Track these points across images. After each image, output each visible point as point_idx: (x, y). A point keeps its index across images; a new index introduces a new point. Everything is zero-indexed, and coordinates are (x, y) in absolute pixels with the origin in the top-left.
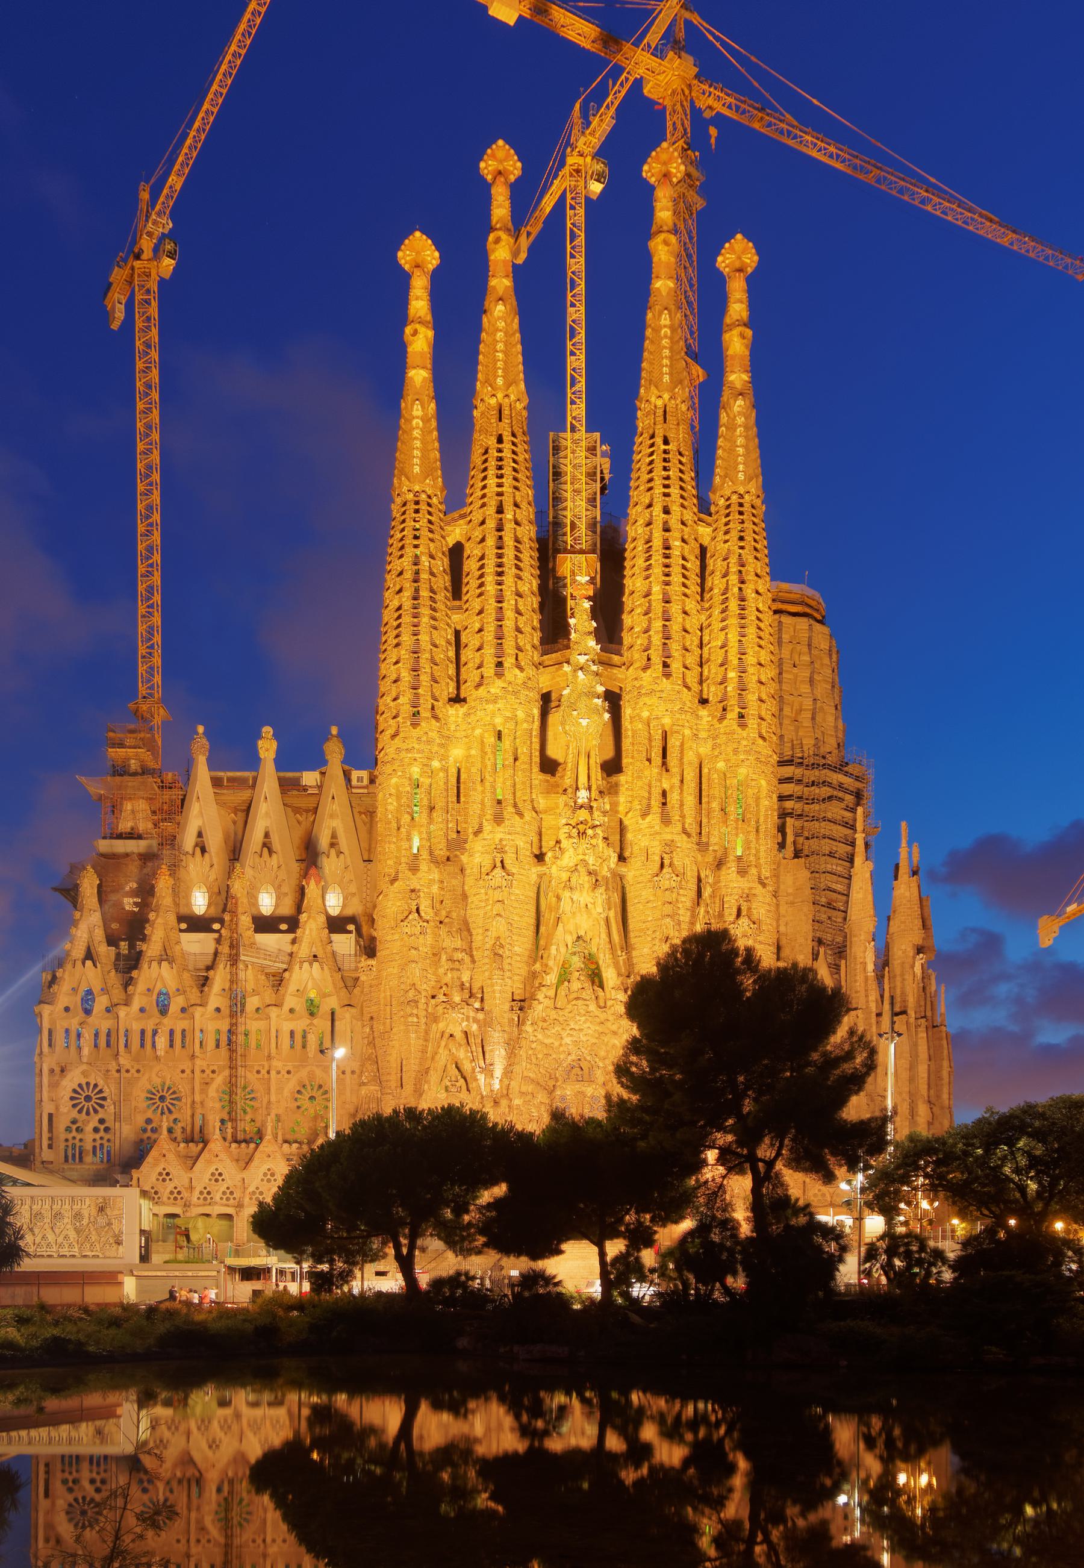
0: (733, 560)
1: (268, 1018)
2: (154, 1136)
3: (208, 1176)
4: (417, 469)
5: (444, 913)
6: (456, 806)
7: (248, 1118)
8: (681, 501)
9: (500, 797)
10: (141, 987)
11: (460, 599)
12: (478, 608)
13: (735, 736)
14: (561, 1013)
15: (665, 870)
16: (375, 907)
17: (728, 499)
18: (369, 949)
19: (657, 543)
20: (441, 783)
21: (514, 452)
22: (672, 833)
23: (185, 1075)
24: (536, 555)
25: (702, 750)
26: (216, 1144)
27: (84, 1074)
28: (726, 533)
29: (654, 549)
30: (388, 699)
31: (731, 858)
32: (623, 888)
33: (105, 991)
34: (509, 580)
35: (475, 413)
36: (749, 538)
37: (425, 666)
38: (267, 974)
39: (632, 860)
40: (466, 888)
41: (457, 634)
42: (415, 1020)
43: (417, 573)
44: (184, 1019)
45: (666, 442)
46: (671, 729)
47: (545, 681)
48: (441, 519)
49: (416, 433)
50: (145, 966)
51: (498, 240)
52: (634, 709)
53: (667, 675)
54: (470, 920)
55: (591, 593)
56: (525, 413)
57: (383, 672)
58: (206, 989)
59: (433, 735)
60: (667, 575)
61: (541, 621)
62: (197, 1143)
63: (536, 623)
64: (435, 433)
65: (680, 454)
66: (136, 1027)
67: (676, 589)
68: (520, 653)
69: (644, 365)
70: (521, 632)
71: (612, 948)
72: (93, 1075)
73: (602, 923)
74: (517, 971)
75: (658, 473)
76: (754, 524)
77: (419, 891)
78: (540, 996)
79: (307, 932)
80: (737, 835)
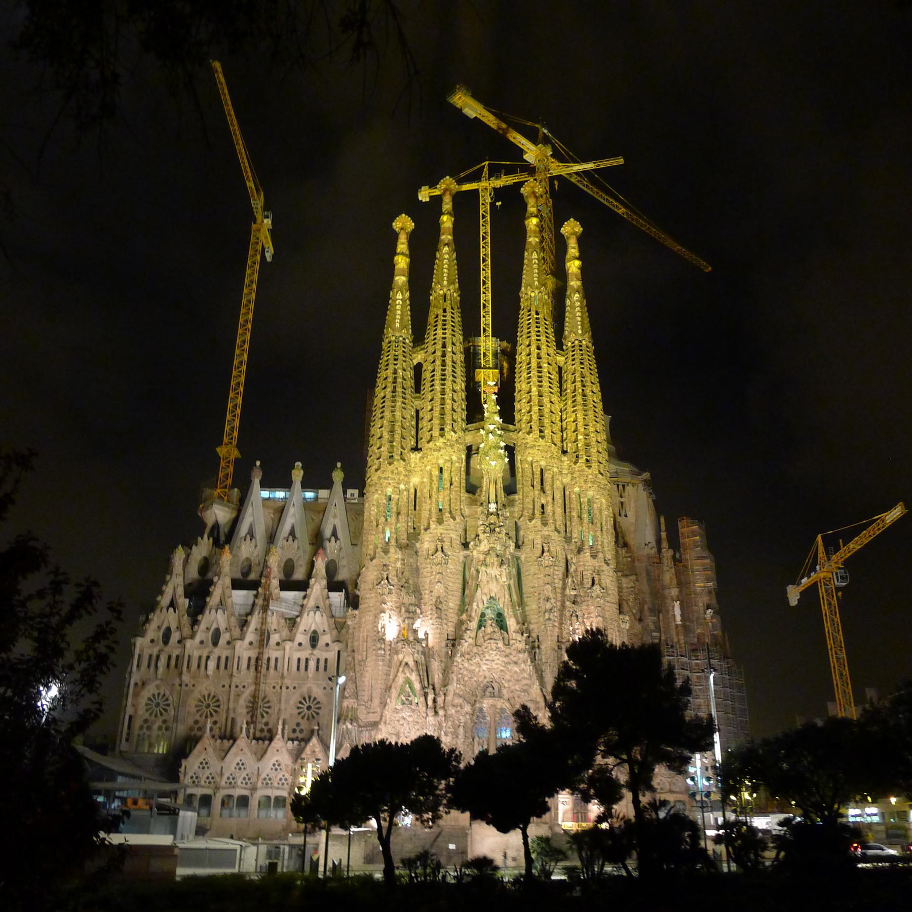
0: (578, 375)
1: (284, 649)
2: (199, 733)
3: (234, 765)
4: (398, 325)
5: (404, 580)
6: (413, 512)
7: (264, 720)
9: (441, 507)
10: (203, 626)
11: (420, 393)
12: (430, 398)
14: (479, 648)
15: (545, 554)
16: (359, 575)
17: (573, 343)
18: (353, 602)
19: (534, 365)
20: (405, 499)
21: (452, 317)
22: (548, 531)
23: (224, 689)
24: (464, 370)
25: (565, 481)
26: (242, 742)
27: (158, 687)
28: (573, 360)
30: (375, 448)
31: (586, 547)
32: (518, 565)
33: (179, 628)
34: (448, 383)
35: (431, 297)
36: (586, 363)
37: (398, 430)
38: (286, 619)
39: (524, 548)
40: (419, 564)
41: (417, 412)
42: (383, 652)
43: (395, 378)
44: (229, 649)
45: (537, 313)
46: (545, 468)
47: (469, 439)
49: (398, 307)
50: (207, 612)
52: (522, 456)
53: (543, 437)
54: (421, 585)
55: (496, 391)
56: (459, 298)
57: (372, 432)
58: (245, 628)
60: (541, 382)
61: (467, 406)
62: (228, 740)
63: (464, 407)
64: (409, 307)
65: (545, 320)
66: (196, 654)
67: (546, 389)
68: (454, 423)
69: (524, 276)
70: (455, 411)
71: (513, 606)
72: (163, 688)
73: (506, 588)
74: (451, 620)
75: (533, 329)
77: (389, 565)
78: (466, 637)
79: (314, 590)
80: (589, 532)
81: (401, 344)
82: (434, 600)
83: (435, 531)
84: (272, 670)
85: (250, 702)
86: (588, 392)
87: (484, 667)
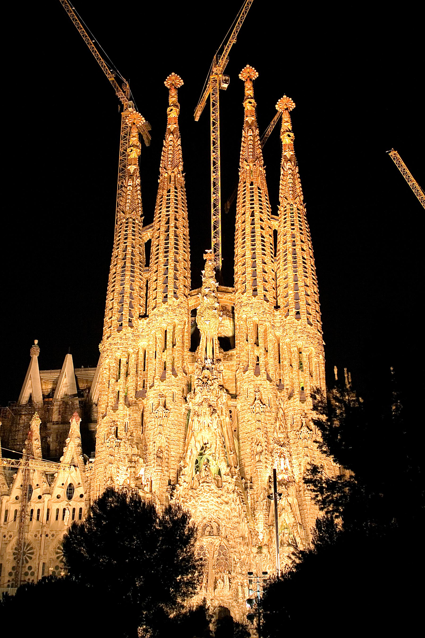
0: (289, 235)
8: (260, 210)
13: (294, 324)
28: (285, 223)
29: (246, 233)
34: (171, 255)
36: (297, 224)
45: (252, 184)
48: (139, 229)
51: (172, 110)
52: (238, 314)
59: (130, 335)
69: (241, 153)
74: (172, 467)
76: (299, 217)
81: (130, 225)
82: (156, 450)
83: (158, 388)
84: (34, 520)
85: (16, 549)
86: (298, 249)
87: (201, 508)
